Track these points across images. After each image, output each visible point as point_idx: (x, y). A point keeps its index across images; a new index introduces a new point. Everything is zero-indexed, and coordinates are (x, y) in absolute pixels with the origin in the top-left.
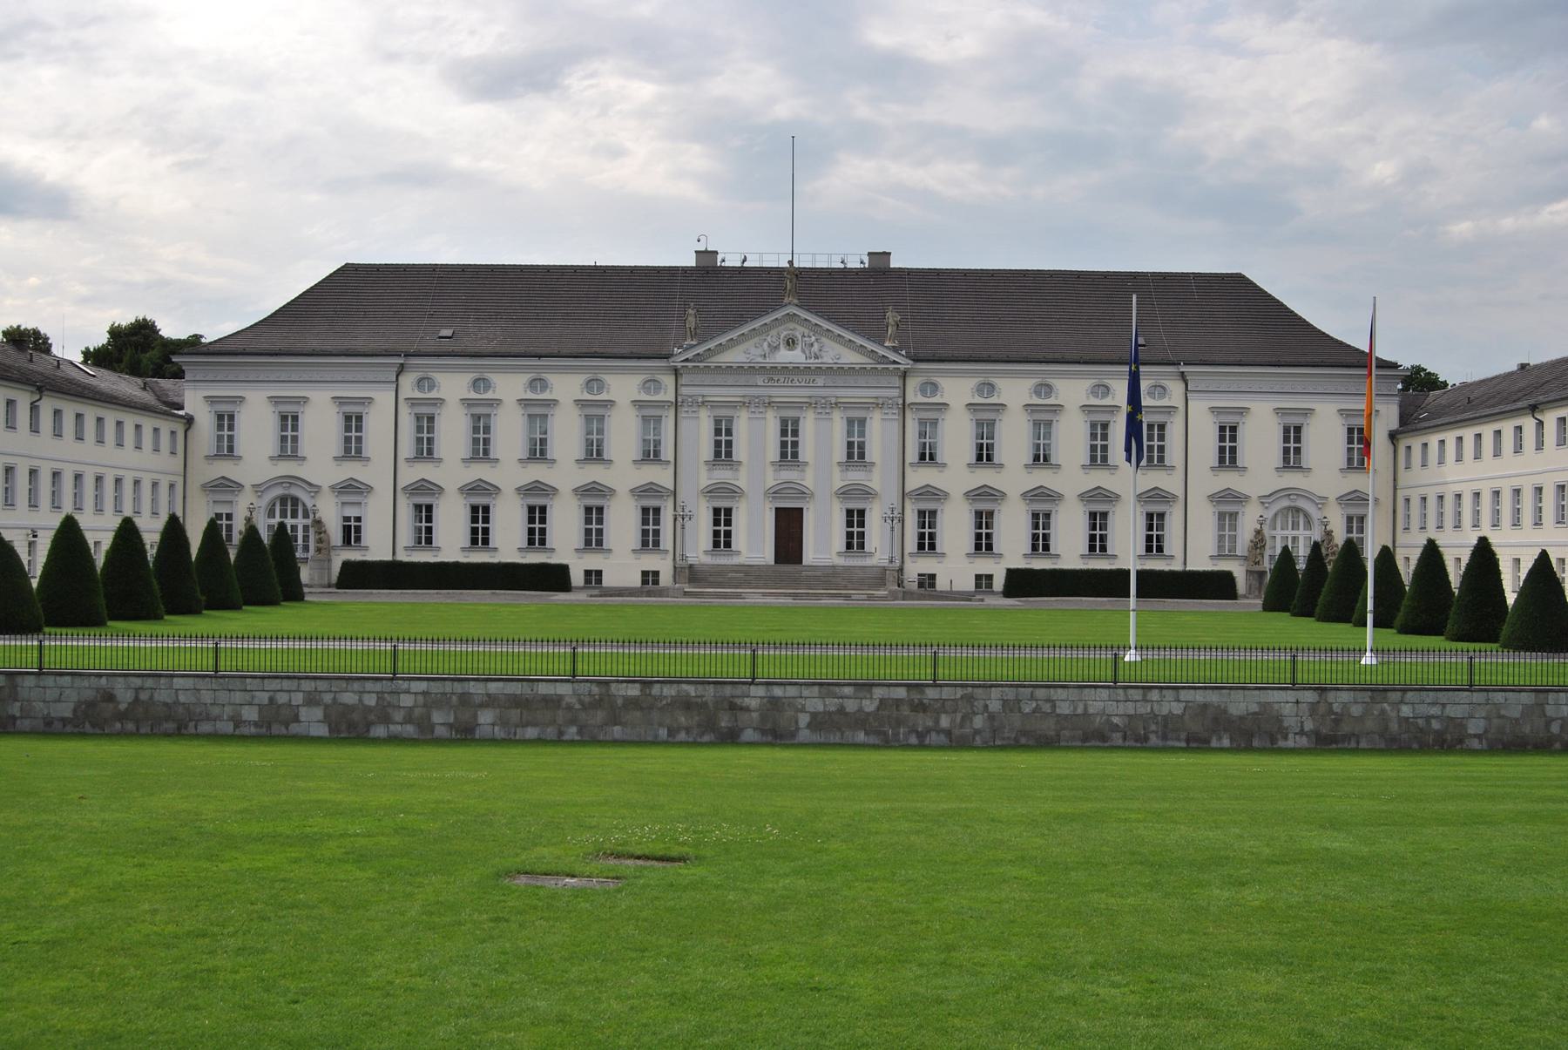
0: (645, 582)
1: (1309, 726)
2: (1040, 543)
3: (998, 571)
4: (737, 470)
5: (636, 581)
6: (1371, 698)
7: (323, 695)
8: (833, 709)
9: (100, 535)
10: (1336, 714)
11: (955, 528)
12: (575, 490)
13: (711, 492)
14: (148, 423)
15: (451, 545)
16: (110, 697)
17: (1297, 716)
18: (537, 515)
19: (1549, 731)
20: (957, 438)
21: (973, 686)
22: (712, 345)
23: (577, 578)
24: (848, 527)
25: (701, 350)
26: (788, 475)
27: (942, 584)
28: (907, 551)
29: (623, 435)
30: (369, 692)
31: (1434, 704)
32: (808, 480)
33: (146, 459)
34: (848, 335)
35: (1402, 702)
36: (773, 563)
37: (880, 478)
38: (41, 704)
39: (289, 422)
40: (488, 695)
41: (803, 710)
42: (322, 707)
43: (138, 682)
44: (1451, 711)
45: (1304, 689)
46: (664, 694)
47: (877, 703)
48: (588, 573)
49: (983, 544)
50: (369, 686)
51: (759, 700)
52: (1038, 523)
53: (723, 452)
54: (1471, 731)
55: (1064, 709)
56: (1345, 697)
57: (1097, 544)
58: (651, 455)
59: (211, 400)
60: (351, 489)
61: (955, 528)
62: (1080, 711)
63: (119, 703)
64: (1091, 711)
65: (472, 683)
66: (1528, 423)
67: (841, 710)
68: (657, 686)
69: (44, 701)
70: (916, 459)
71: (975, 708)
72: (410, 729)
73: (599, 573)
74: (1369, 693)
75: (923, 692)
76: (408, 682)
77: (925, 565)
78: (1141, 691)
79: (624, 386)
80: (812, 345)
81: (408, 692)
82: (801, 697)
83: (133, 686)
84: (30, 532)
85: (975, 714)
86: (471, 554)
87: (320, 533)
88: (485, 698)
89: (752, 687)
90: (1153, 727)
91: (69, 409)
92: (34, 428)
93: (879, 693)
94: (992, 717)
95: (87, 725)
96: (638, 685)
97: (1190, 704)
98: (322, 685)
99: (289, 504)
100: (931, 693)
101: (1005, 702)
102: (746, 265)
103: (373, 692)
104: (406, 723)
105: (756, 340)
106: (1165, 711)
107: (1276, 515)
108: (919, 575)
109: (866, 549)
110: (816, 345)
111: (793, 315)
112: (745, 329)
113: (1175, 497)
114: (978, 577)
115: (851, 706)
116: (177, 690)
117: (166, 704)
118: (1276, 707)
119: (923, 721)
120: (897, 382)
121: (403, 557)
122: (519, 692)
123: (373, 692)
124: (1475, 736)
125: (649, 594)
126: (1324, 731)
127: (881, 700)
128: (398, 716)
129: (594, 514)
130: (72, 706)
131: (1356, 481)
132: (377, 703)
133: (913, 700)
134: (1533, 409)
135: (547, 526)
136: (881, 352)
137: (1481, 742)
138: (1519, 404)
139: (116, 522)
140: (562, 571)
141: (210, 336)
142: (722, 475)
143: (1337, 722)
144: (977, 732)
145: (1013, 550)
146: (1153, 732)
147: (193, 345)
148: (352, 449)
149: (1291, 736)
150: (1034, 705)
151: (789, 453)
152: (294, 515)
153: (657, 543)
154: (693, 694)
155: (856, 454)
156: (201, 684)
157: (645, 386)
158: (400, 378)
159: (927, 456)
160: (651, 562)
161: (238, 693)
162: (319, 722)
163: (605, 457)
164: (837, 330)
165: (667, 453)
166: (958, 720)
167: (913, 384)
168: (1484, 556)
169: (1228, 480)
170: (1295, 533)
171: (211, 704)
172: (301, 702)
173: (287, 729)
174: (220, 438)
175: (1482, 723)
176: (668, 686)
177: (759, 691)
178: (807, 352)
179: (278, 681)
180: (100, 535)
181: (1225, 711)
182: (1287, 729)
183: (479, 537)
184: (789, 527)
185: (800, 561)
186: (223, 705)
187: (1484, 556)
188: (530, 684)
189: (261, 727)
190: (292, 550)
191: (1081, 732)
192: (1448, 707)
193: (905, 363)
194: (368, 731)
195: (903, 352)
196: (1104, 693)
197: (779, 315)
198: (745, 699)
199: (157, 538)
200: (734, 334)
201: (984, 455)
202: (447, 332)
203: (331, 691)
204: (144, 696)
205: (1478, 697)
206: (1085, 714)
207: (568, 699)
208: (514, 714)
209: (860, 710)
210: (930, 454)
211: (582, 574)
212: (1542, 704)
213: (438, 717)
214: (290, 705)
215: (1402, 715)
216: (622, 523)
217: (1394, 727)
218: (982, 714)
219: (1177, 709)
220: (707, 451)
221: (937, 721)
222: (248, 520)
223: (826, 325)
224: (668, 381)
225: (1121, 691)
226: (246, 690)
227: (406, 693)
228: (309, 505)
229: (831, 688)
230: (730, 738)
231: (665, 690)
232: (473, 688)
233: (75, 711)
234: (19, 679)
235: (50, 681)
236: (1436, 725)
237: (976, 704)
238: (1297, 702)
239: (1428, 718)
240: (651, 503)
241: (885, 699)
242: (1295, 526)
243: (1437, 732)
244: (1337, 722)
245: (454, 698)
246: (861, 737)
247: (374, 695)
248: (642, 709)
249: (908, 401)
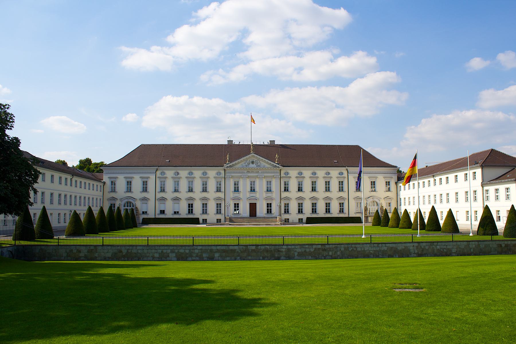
0: (217, 222)
1: (416, 252)
2: (314, 211)
3: (304, 217)
4: (240, 194)
5: (216, 221)
6: (430, 244)
7: (175, 250)
8: (303, 251)
9: (96, 212)
10: (422, 248)
11: (294, 207)
12: (200, 199)
13: (233, 199)
14: (96, 183)
16: (121, 251)
17: (413, 249)
19: (470, 251)
20: (293, 186)
21: (337, 244)
22: (234, 163)
23: (201, 221)
24: (267, 207)
25: (231, 164)
26: (253, 194)
27: (290, 221)
28: (282, 213)
29: (212, 186)
30: (187, 249)
31: (445, 245)
32: (257, 195)
33: (95, 193)
34: (267, 161)
35: (437, 245)
36: (249, 216)
37: (275, 195)
38: (103, 254)
39: (129, 183)
40: (217, 249)
41: (296, 251)
42: (175, 253)
43: (128, 247)
44: (448, 247)
45: (415, 243)
46: (261, 248)
47: (314, 249)
48: (203, 220)
49: (300, 211)
50: (187, 248)
51: (285, 249)
52: (313, 206)
53: (236, 190)
54: (453, 252)
55: (359, 249)
56: (424, 244)
57: (328, 211)
58: (218, 190)
59: (110, 178)
60: (145, 200)
61: (294, 207)
62: (362, 250)
63: (123, 253)
64: (365, 250)
65: (213, 246)
66: (432, 180)
67: (305, 251)
68: (260, 246)
69: (104, 253)
71: (338, 250)
72: (197, 258)
73: (206, 220)
74: (430, 243)
75: (325, 246)
76: (197, 246)
77: (286, 216)
78: (377, 244)
79: (212, 173)
80: (258, 163)
81: (197, 249)
82: (295, 248)
83: (127, 248)
84: (70, 211)
85: (338, 251)
86: (174, 215)
87: (137, 211)
88: (216, 250)
89: (283, 246)
90: (380, 253)
91: (79, 179)
92: (71, 185)
93: (314, 247)
94: (342, 252)
95: (115, 258)
96: (255, 246)
97: (389, 247)
98: (175, 248)
99: (129, 203)
100: (327, 246)
101: (345, 248)
102: (240, 144)
103: (188, 249)
104: (197, 257)
105: (244, 162)
106: (383, 249)
107: (370, 203)
108: (285, 219)
109: (272, 213)
110: (259, 163)
111: (252, 156)
112: (242, 159)
113: (346, 199)
114: (299, 219)
115: (308, 250)
116: (138, 249)
117: (135, 253)
118: (409, 247)
119: (325, 253)
120: (279, 172)
121: (157, 217)
122: (225, 249)
123: (188, 249)
124: (454, 253)
125: (221, 225)
126: (420, 253)
127: (315, 248)
128: (194, 255)
129: (205, 206)
130: (111, 253)
131: (388, 194)
132: (189, 252)
133: (322, 248)
134: (433, 176)
135: (193, 208)
136: (275, 164)
137: (455, 254)
138: (430, 175)
139: (99, 208)
140: (198, 219)
141: (107, 162)
142: (236, 194)
143: (423, 250)
144: (339, 256)
145: (308, 212)
146: (380, 254)
147: (102, 164)
148: (145, 189)
149: (412, 254)
150: (352, 249)
153: (220, 213)
154: (269, 248)
155: (269, 190)
156: (144, 248)
157: (217, 174)
158: (157, 172)
159: (286, 190)
160: (219, 217)
161: (153, 250)
162: (174, 257)
163: (207, 191)
164: (264, 159)
165: (223, 190)
166: (334, 253)
167: (282, 172)
168: (433, 211)
169: (358, 194)
171: (147, 253)
172: (169, 252)
173: (166, 259)
174: (112, 187)
175: (456, 250)
176: (262, 246)
177: (285, 247)
178: (257, 165)
179: (164, 247)
180: (96, 212)
181: (397, 249)
182: (411, 252)
184: (253, 207)
185: (256, 216)
186: (150, 253)
187: (433, 211)
188: (228, 246)
189: (160, 258)
191: (363, 255)
192: (448, 246)
193: (281, 167)
194: (187, 259)
195: (280, 165)
196: (368, 245)
197: (250, 155)
198: (282, 249)
199: (97, 212)
200: (239, 160)
201: (300, 189)
202: (168, 161)
203: (177, 249)
204: (129, 251)
205: (454, 243)
206: (364, 250)
207: (237, 250)
208: (224, 254)
209: (310, 251)
210: (287, 189)
211: (202, 220)
212: (469, 245)
213: (204, 255)
214: (167, 253)
215: (437, 248)
216: (212, 207)
217: (436, 251)
218: (339, 251)
219: (386, 248)
220: (232, 189)
221: (329, 253)
222: (118, 208)
223: (261, 158)
224: (223, 172)
225: (372, 245)
226: (155, 249)
227: (196, 249)
228: (134, 204)
229: (303, 246)
230: (278, 259)
231: (262, 247)
232: (213, 248)
233: (112, 255)
234: (97, 247)
235: (105, 247)
236: (445, 250)
237: (338, 249)
238: (413, 246)
239: (443, 249)
240: (219, 202)
241: (316, 248)
243: (445, 252)
244: (423, 250)
245: (209, 250)
246: (310, 257)
247: (188, 250)
248: (256, 252)
249: (281, 177)
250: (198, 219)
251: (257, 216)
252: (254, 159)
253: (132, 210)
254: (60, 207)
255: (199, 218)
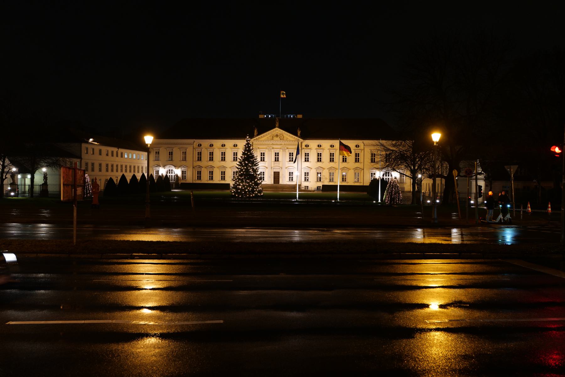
2: (331, 180)
3: (320, 184)
11: (313, 177)
15: (205, 179)
18: (223, 173)
20: (313, 157)
25: (257, 137)
28: (302, 181)
70: (304, 161)
109: (293, 181)
121: (194, 182)
140: (229, 184)
151: (277, 160)
152: (172, 173)
170: (389, 177)
183: (211, 178)
184: (277, 176)
190: (169, 180)
193: (301, 140)
242: (389, 176)
250: (229, 184)
251: (280, 183)
252: (278, 133)
253: (167, 175)
254: (107, 173)
255: (230, 184)
